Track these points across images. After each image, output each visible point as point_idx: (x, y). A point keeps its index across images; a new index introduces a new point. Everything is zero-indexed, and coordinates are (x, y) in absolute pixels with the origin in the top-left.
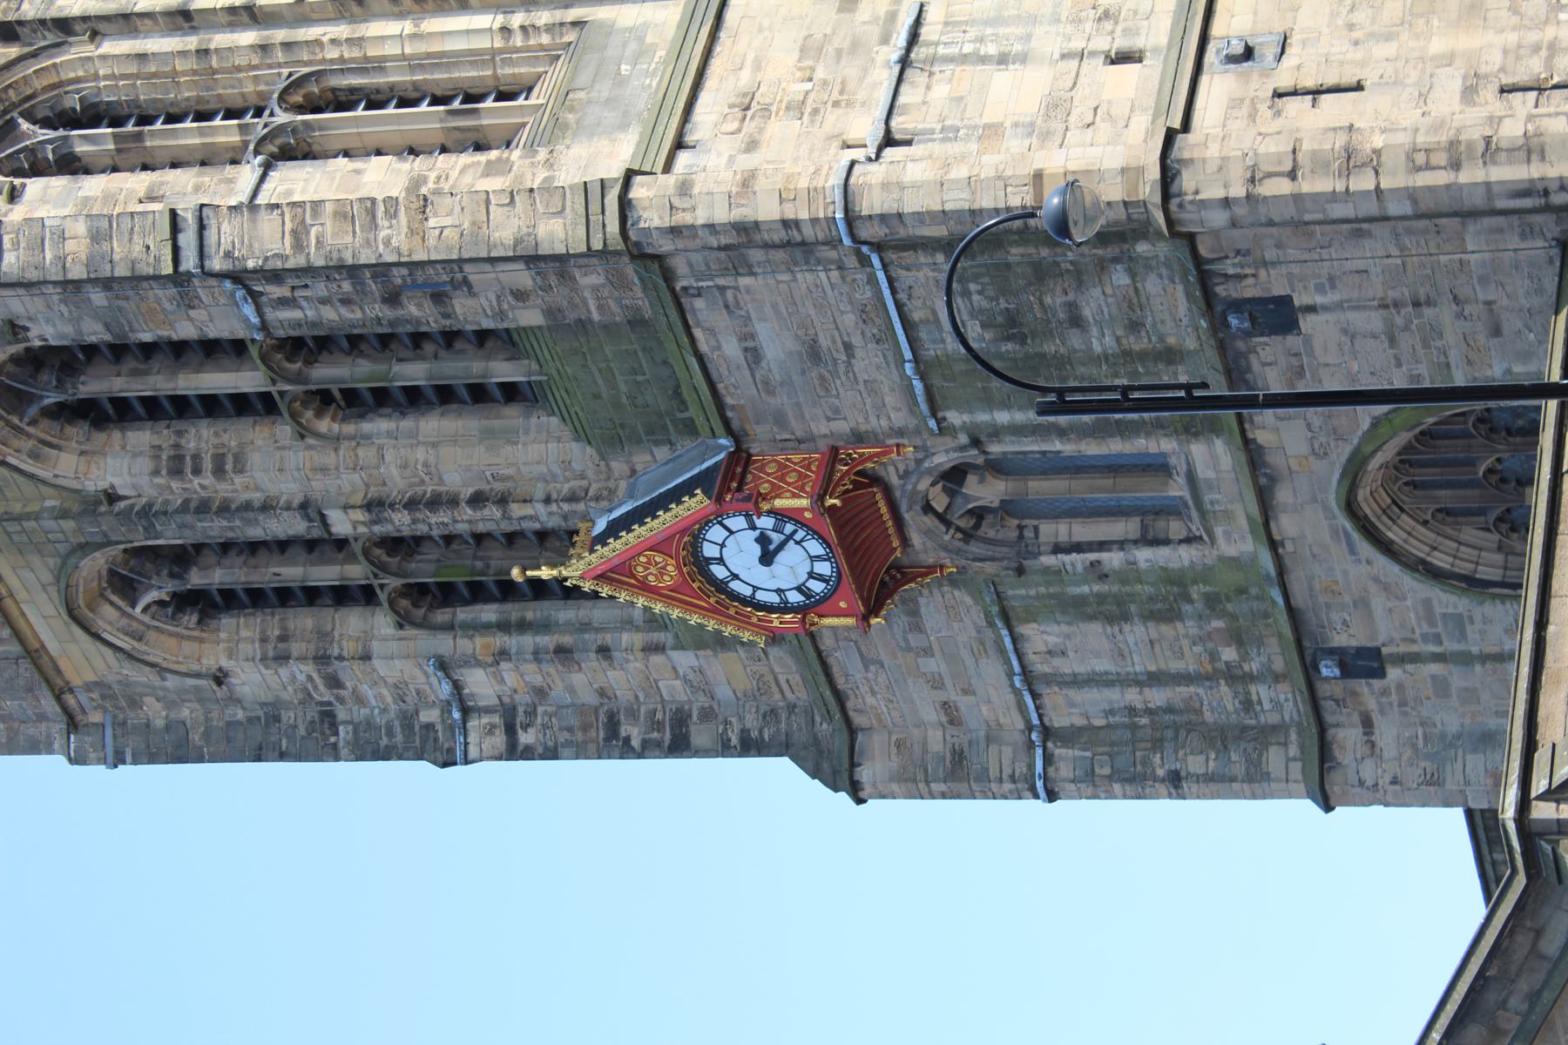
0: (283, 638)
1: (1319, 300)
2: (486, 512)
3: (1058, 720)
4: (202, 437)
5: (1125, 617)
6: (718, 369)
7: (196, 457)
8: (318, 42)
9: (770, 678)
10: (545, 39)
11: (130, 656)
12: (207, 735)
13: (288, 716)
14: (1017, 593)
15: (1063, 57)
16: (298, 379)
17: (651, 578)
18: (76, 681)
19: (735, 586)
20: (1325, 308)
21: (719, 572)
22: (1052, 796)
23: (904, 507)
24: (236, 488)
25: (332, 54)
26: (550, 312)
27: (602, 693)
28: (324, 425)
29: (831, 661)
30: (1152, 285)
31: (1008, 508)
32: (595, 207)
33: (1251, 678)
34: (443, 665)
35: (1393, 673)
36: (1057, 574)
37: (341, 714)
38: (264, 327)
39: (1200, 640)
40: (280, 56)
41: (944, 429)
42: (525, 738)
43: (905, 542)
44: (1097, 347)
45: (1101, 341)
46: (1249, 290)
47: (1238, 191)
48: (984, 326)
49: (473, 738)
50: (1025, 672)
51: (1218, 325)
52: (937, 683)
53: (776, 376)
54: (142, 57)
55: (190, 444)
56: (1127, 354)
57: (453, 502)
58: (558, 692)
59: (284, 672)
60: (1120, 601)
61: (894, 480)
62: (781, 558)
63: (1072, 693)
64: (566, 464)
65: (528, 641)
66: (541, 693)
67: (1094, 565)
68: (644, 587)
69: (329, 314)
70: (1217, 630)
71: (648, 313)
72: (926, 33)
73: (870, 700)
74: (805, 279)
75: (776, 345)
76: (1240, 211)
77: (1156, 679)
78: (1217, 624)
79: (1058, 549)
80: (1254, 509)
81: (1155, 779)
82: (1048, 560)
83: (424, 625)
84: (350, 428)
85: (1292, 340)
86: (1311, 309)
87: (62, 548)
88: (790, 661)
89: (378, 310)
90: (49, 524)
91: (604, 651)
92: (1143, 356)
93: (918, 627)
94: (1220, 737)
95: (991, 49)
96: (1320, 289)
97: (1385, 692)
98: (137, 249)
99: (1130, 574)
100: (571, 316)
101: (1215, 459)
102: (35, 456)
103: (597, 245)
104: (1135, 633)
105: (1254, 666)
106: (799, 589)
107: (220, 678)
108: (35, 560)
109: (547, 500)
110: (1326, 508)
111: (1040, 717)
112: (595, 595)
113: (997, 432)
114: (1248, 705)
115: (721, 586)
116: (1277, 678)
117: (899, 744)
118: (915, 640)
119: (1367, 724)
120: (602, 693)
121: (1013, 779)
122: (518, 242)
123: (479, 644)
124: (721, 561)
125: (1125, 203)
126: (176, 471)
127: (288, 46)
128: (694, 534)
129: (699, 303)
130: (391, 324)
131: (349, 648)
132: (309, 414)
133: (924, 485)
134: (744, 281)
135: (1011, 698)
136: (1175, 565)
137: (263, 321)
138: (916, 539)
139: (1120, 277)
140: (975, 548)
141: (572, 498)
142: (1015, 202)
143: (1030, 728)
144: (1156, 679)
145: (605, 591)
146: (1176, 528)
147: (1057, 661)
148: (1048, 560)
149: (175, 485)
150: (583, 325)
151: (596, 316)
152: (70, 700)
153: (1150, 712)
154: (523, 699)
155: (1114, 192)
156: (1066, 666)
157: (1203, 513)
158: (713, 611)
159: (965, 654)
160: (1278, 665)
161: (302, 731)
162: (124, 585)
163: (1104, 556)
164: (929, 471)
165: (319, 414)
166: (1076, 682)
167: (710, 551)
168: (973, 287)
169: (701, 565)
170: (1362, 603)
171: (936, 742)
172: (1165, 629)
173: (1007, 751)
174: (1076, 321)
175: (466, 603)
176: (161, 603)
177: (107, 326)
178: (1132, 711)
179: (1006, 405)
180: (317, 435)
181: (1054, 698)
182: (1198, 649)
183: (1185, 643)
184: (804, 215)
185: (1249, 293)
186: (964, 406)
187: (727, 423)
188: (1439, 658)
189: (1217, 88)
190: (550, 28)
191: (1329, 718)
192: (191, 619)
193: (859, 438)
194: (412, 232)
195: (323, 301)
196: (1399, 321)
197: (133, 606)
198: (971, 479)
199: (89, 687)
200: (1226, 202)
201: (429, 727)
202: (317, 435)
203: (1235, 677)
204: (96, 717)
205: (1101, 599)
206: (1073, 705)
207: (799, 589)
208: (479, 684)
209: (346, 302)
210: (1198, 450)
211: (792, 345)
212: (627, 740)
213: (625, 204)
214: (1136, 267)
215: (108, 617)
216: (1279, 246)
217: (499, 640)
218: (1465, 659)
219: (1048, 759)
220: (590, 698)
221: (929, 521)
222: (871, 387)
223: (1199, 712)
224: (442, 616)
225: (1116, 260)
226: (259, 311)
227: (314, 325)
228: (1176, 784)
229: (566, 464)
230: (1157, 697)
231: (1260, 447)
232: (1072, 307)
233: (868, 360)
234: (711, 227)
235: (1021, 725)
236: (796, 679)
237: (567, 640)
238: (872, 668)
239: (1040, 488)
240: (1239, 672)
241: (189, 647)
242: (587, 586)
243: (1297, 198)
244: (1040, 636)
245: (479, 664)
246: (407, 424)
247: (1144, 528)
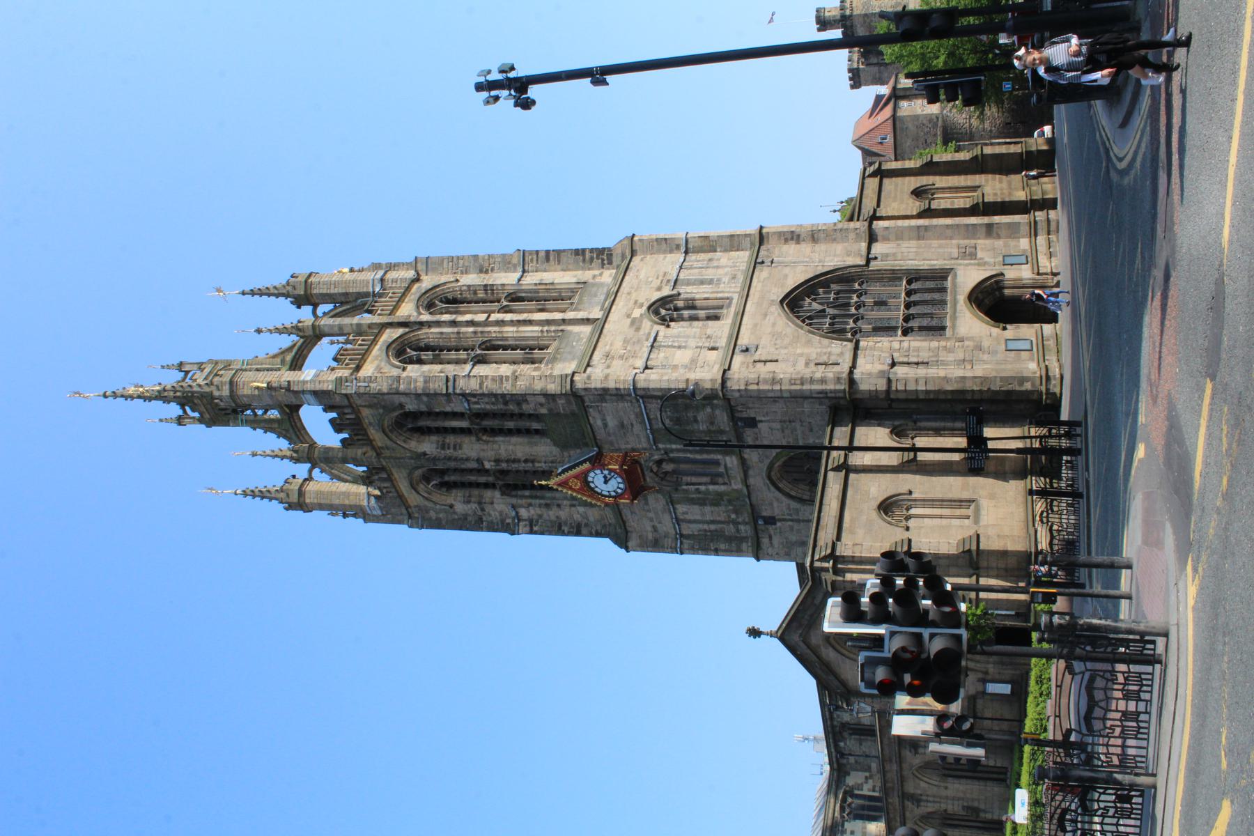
0: (470, 496)
1: (763, 419)
3: (685, 532)
4: (451, 439)
5: (706, 505)
6: (596, 428)
7: (449, 444)
8: (490, 332)
10: (553, 334)
11: (426, 499)
12: (447, 523)
13: (470, 518)
14: (675, 496)
15: (697, 347)
16: (477, 424)
18: (412, 505)
19: (596, 489)
20: (765, 421)
21: (592, 485)
22: (682, 553)
23: (645, 469)
24: (459, 453)
25: (494, 335)
26: (550, 410)
27: (557, 517)
28: (484, 438)
30: (717, 412)
31: (674, 472)
32: (564, 381)
33: (739, 523)
34: (514, 507)
35: (779, 524)
36: (686, 491)
37: (484, 519)
38: (470, 409)
39: (727, 511)
40: (479, 335)
41: (658, 449)
42: (535, 528)
43: (645, 480)
44: (701, 428)
45: (703, 427)
46: (744, 415)
47: (743, 387)
48: (671, 421)
49: (520, 528)
50: (677, 519)
51: (735, 424)
52: (651, 520)
53: (611, 431)
54: (442, 333)
55: (447, 441)
56: (709, 431)
57: (518, 461)
58: (545, 516)
59: (469, 506)
60: (704, 500)
61: (643, 462)
62: (610, 482)
64: (551, 453)
65: (538, 501)
66: (540, 516)
67: (697, 489)
68: (571, 488)
69: (488, 407)
71: (577, 412)
72: (659, 339)
74: (621, 405)
75: (612, 423)
76: (743, 393)
77: (713, 522)
78: (731, 507)
79: (687, 484)
80: (742, 475)
81: (711, 550)
82: (685, 487)
83: (508, 495)
84: (491, 439)
85: (756, 430)
86: (761, 421)
87: (410, 467)
88: (611, 512)
89: (501, 406)
90: (407, 460)
91: (559, 506)
92: (714, 432)
93: (647, 504)
94: (729, 539)
95: (676, 344)
96: (764, 416)
97: (776, 529)
98: (437, 386)
99: (707, 492)
101: (732, 462)
102: (405, 441)
103: (564, 392)
104: (708, 509)
105: (740, 520)
106: (614, 491)
107: (451, 506)
108: (403, 471)
109: (545, 463)
112: (557, 490)
113: (672, 451)
114: (738, 531)
115: (592, 489)
116: (746, 523)
117: (640, 536)
118: (646, 507)
119: (770, 538)
120: (557, 517)
121: (671, 548)
122: (542, 390)
123: (523, 501)
124: (593, 482)
125: (712, 389)
126: (443, 448)
127: (482, 332)
128: (585, 474)
129: (591, 410)
131: (487, 500)
132: (481, 434)
133: (651, 464)
134: (604, 404)
135: (671, 525)
138: (648, 479)
139: (709, 410)
140: (664, 483)
141: (552, 462)
142: (681, 387)
143: (676, 533)
144: (713, 522)
145: (560, 489)
146: (720, 480)
148: (685, 487)
149: (443, 452)
150: (558, 414)
151: (562, 412)
152: (410, 510)
153: (710, 531)
154: (535, 517)
155: (708, 386)
156: (689, 517)
157: (728, 476)
158: (589, 496)
159: (660, 513)
160: (747, 520)
161: (473, 523)
162: (426, 479)
163: (700, 487)
164: (653, 460)
165: (483, 435)
166: (690, 522)
167: (590, 479)
168: (668, 410)
169: (587, 483)
170: (771, 504)
171: (650, 536)
172: (716, 508)
173: (670, 540)
174: (696, 421)
175: (521, 490)
176: (436, 484)
177: (427, 407)
178: (705, 531)
179: (675, 443)
180: (482, 440)
181: (684, 526)
184: (622, 387)
185: (746, 416)
187: (596, 443)
188: (792, 520)
189: (738, 359)
190: (554, 331)
191: (760, 536)
192: (444, 489)
193: (633, 450)
194: (512, 385)
195: (487, 403)
196: (785, 426)
197: (429, 484)
198: (664, 463)
199: (415, 506)
200: (739, 390)
201: (508, 524)
202: (482, 440)
203: (735, 523)
204: (416, 515)
205: (699, 499)
206: (689, 528)
207: (614, 491)
208: (524, 513)
209: (493, 404)
210: (728, 459)
211: (616, 423)
212: (564, 531)
213: (572, 381)
214: (713, 407)
215: (421, 487)
216: (753, 403)
217: (529, 501)
218: (798, 521)
219: (681, 543)
220: (553, 518)
221: (652, 474)
222: (638, 436)
224: (514, 493)
225: (708, 405)
226: (469, 405)
227: (483, 410)
228: (717, 552)
229: (551, 453)
230: (713, 527)
231: (745, 459)
232: (695, 417)
233: (637, 428)
234: (596, 389)
235: (674, 533)
236: (612, 516)
237: (548, 502)
239: (683, 467)
241: (443, 497)
242: (555, 487)
243: (759, 390)
244: (681, 508)
245: (524, 507)
246: (507, 439)
247: (712, 479)
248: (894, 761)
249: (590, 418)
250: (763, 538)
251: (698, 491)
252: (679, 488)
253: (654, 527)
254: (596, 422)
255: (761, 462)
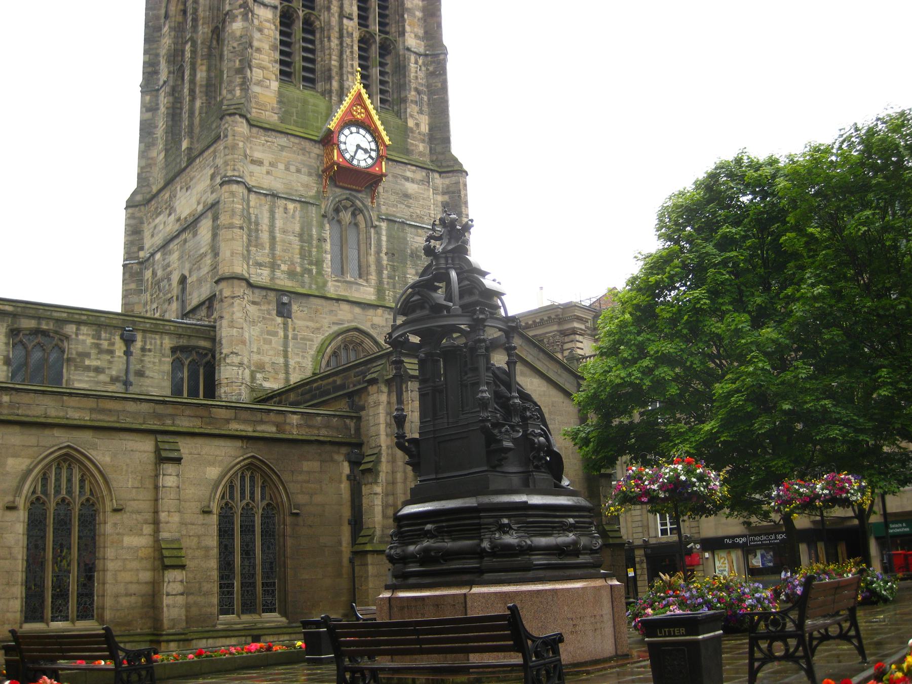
2: (349, 67)
5: (302, 240)
6: (402, 167)
9: (263, 108)
17: (355, 108)
19: (346, 132)
21: (354, 129)
26: (411, 129)
29: (283, 135)
33: (273, 271)
34: (275, 7)
35: (279, 320)
36: (321, 226)
48: (416, 248)
52: (271, 164)
61: (359, 195)
63: (267, 207)
66: (260, 30)
67: (325, 240)
68: (352, 105)
69: (413, 70)
70: (296, 268)
73: (263, 138)
75: (411, 188)
77: (273, 238)
89: (413, 86)
93: (298, 171)
97: (269, 314)
99: (319, 248)
100: (410, 134)
101: (369, 294)
104: (295, 241)
105: (278, 273)
110: (352, 321)
111: (256, 192)
113: (378, 234)
114: (259, 265)
116: (272, 279)
118: (293, 169)
119: (254, 303)
120: (258, 50)
129: (424, 174)
130: (409, 85)
136: (325, 266)
137: (411, 51)
144: (273, 238)
147: (281, 209)
153: (257, 230)
156: (279, 213)
160: (278, 282)
167: (362, 131)
169: (359, 124)
170: (311, 319)
172: (297, 251)
178: (257, 224)
179: (388, 241)
182: (287, 258)
183: (290, 255)
186: (388, 230)
188: (286, 337)
191: (257, 291)
195: (416, 72)
203: (273, 266)
205: (311, 236)
210: (372, 290)
211: (410, 191)
218: (286, 345)
221: (344, 197)
222: (393, 206)
223: (256, 246)
230: (265, 236)
238: (280, 147)
240: (276, 267)
248: (94, 416)
249: (414, 168)
250: (253, 293)
251: (321, 240)
252: (326, 221)
253: (260, 163)
254: (409, 170)
255: (373, 326)
